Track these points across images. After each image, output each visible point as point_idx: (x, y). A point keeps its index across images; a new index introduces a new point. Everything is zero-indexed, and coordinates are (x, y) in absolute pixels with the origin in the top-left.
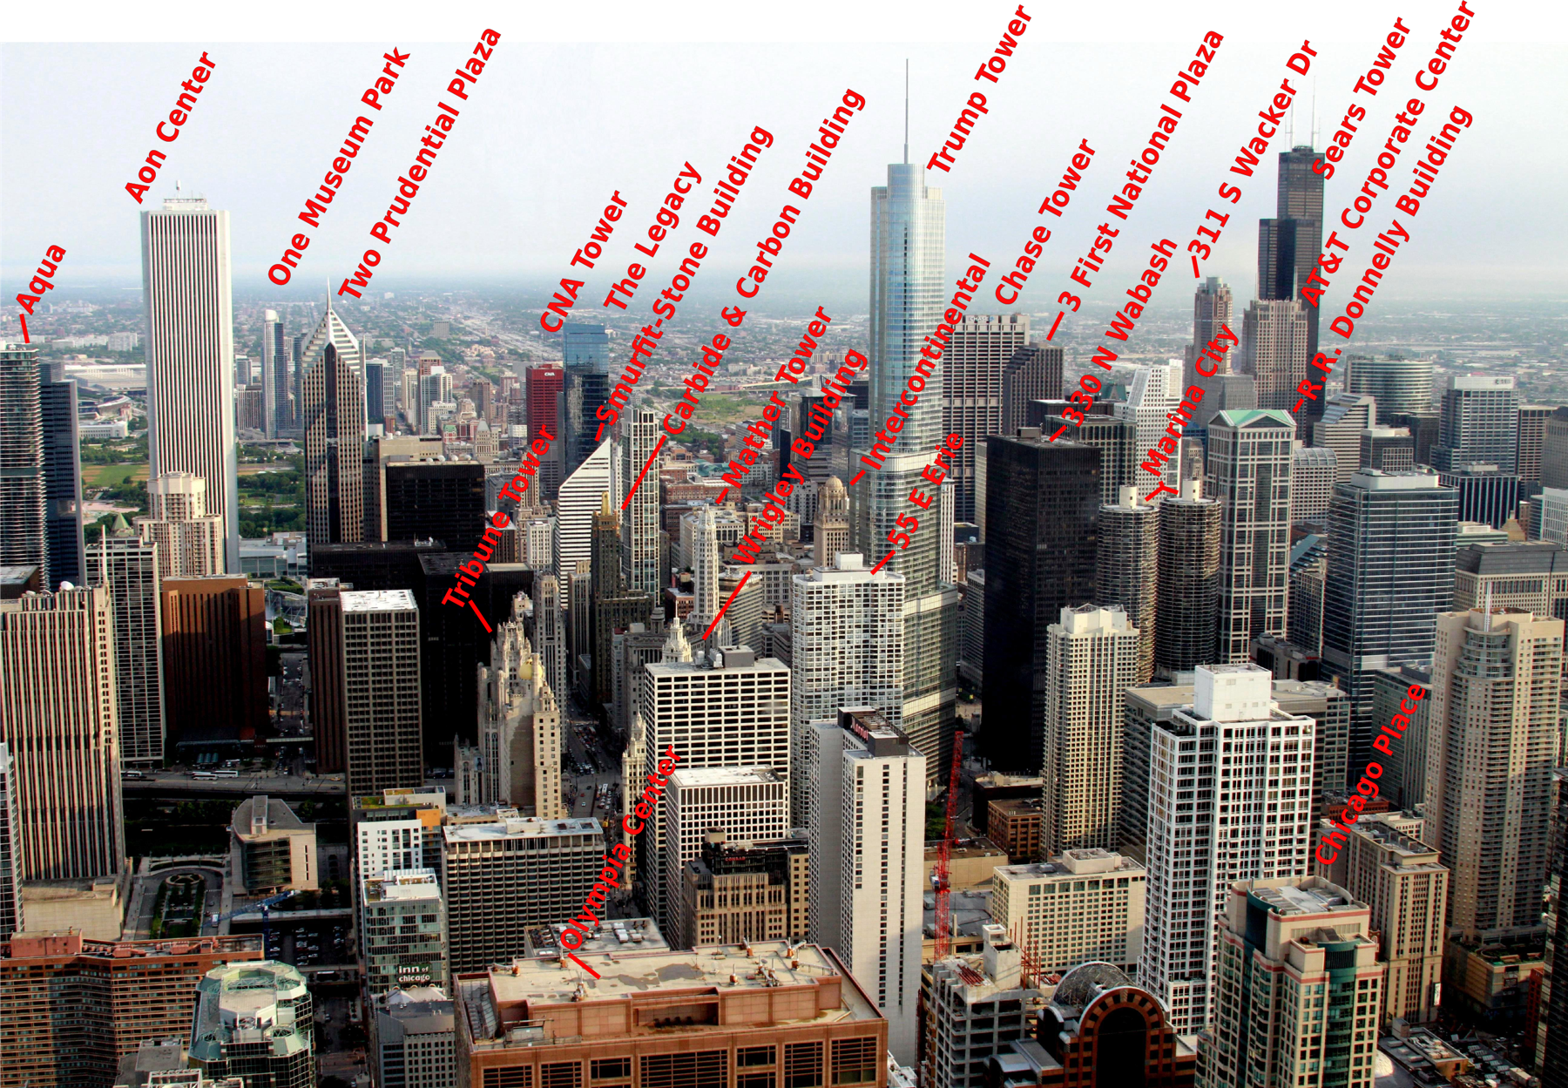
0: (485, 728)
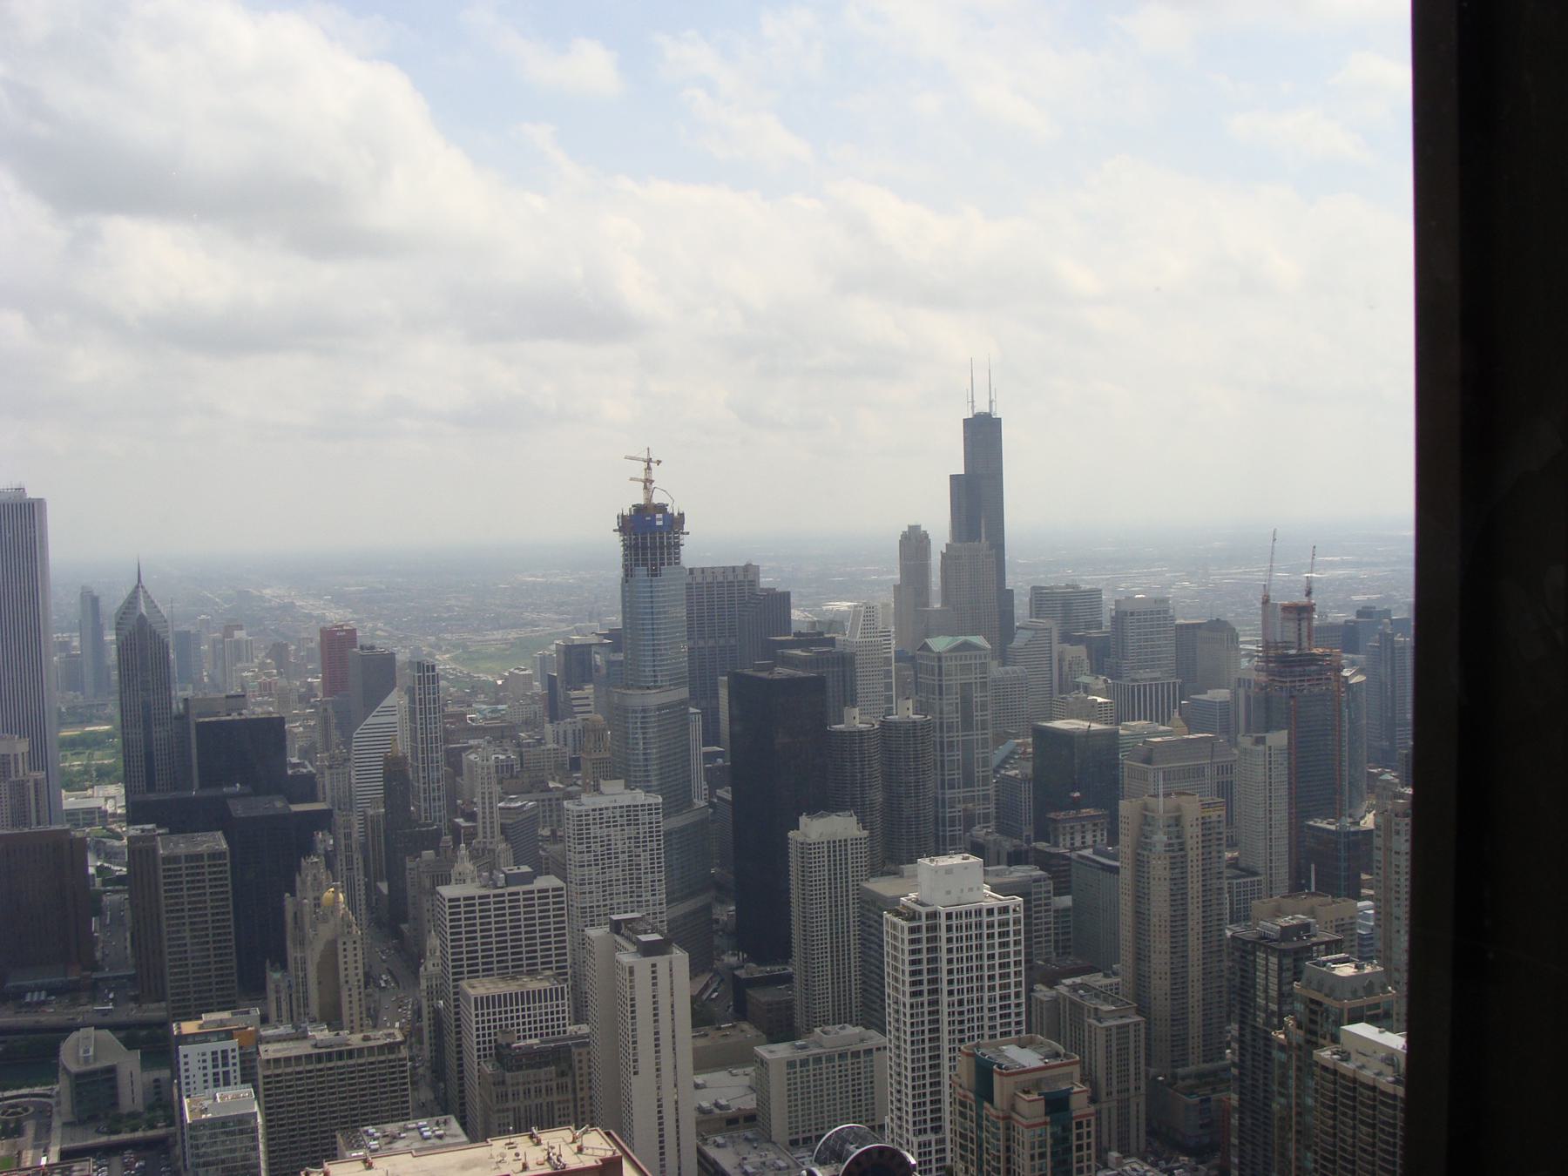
0: (293, 953)
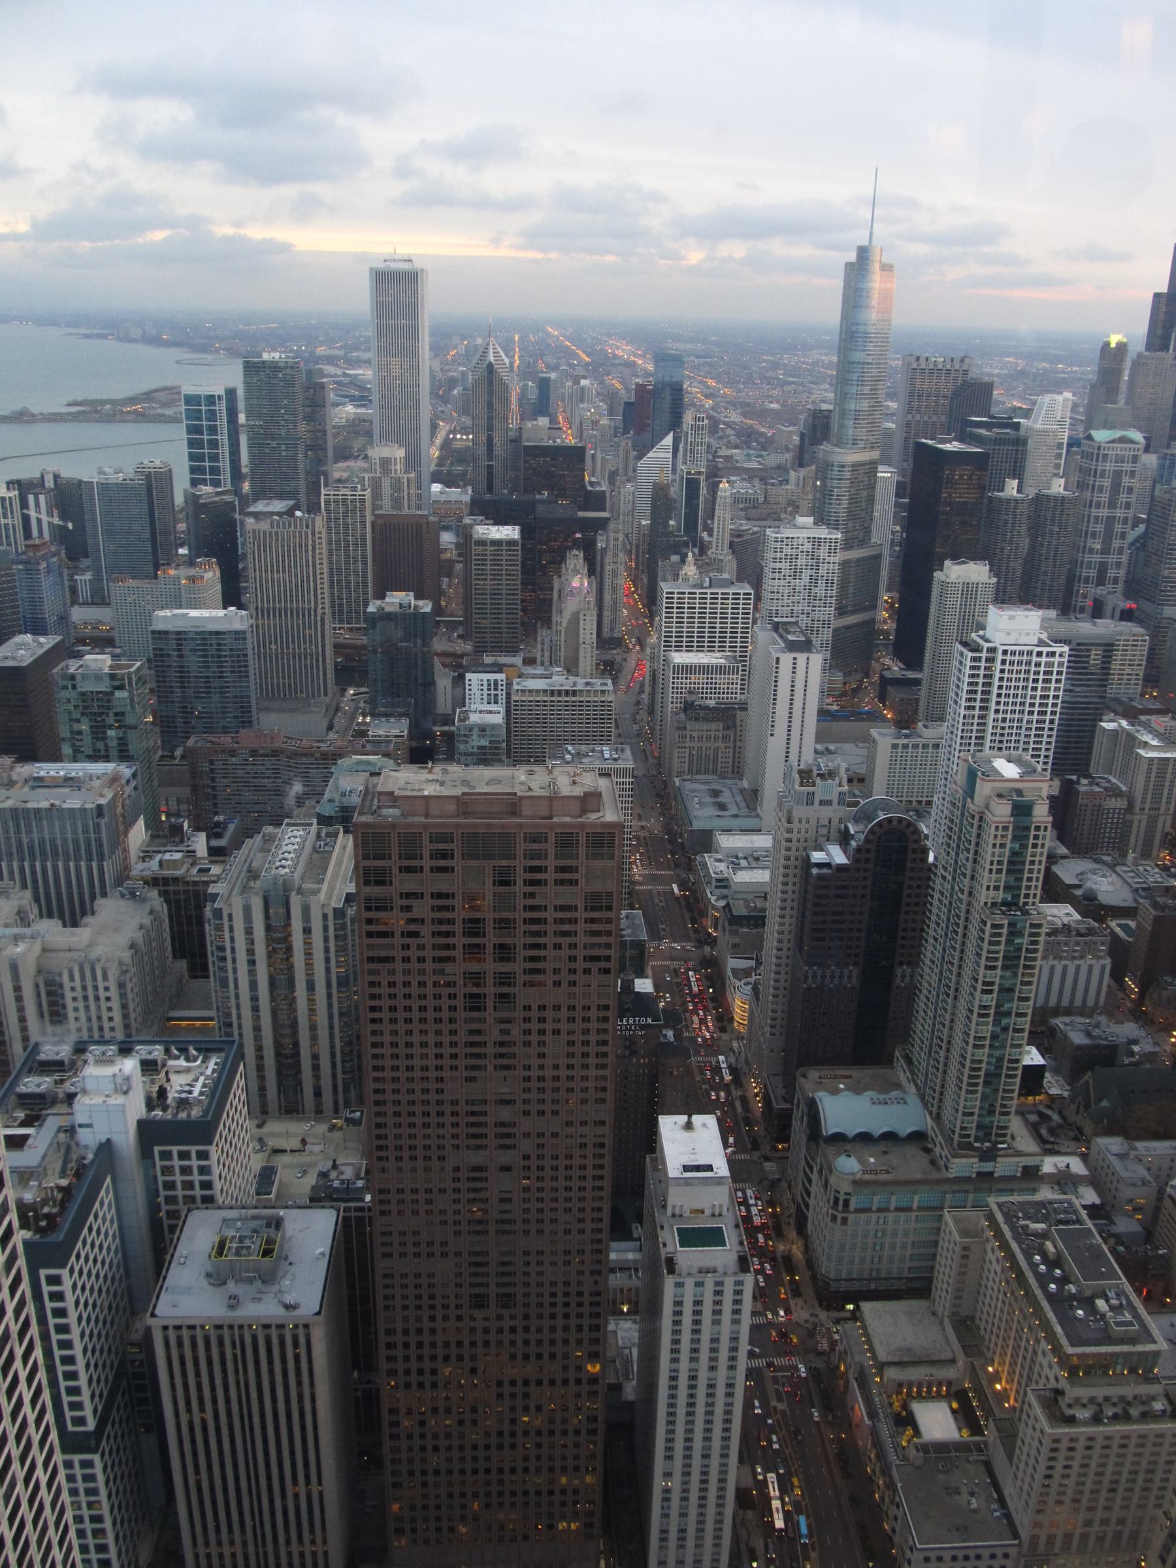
0: (554, 619)
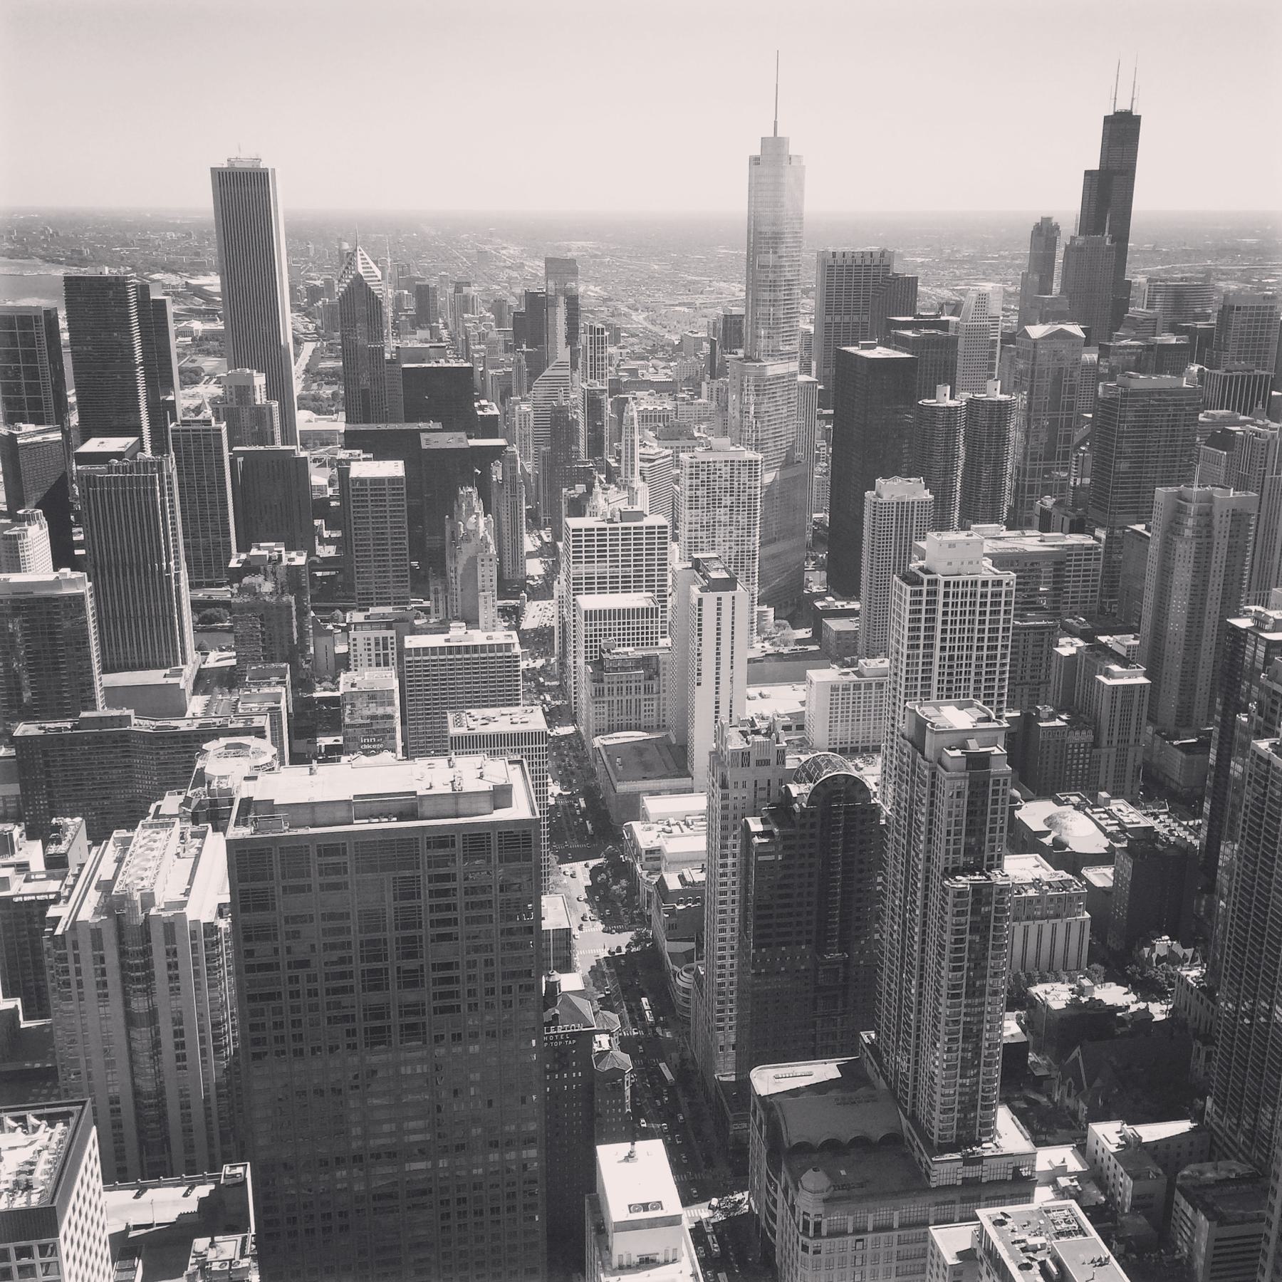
0: (450, 564)
